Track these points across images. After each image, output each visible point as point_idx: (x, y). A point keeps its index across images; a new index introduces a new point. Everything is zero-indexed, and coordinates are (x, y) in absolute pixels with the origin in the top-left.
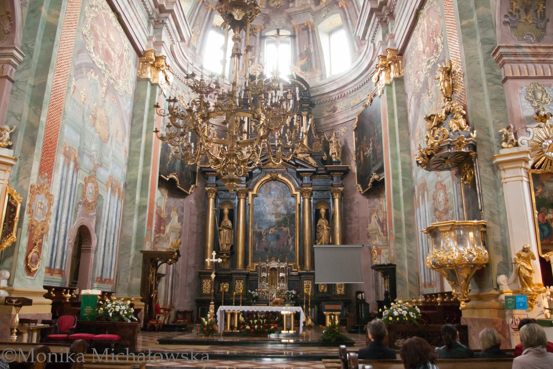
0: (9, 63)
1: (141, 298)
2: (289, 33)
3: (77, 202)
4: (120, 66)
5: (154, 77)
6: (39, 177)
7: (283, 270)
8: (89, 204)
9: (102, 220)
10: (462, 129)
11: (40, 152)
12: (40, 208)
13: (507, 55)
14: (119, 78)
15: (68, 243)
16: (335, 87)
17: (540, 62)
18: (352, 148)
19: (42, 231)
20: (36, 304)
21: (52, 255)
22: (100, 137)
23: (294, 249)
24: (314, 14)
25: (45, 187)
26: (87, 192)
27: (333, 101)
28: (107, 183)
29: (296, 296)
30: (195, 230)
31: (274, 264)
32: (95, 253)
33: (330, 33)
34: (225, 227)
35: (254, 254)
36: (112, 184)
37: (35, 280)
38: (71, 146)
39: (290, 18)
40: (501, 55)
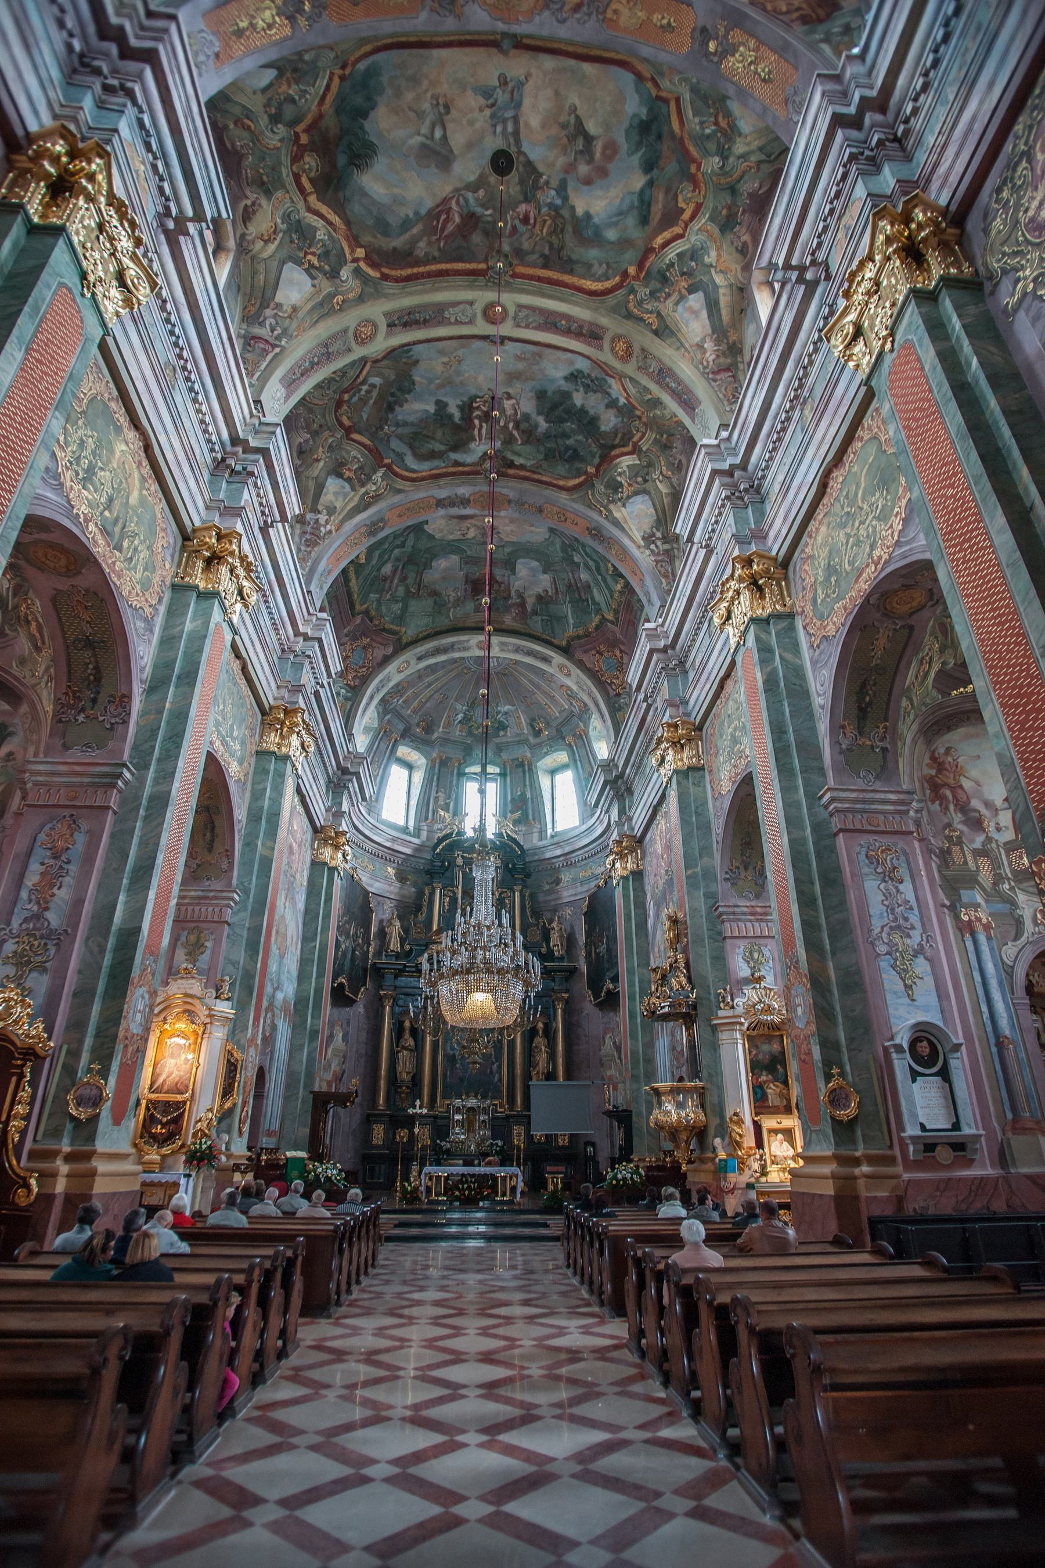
0: (228, 906)
2: (498, 770)
5: (332, 858)
7: (485, 1111)
10: (682, 988)
13: (726, 913)
16: (558, 852)
17: (757, 920)
18: (581, 939)
23: (500, 1080)
24: (532, 747)
27: (557, 870)
29: (502, 1147)
30: (363, 1052)
31: (472, 1102)
33: (553, 772)
34: (404, 1048)
35: (445, 1086)
39: (499, 749)
40: (721, 914)
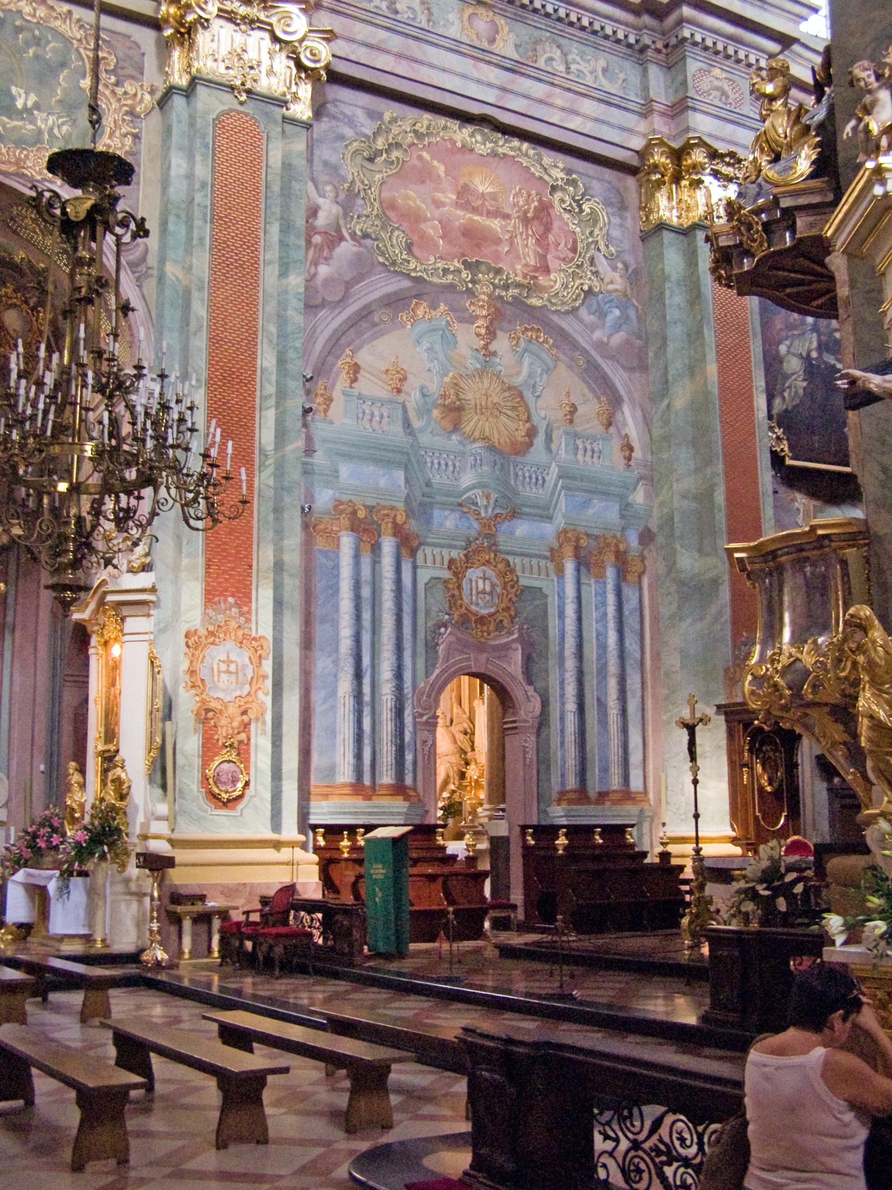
1: (733, 834)
3: (430, 624)
4: (542, 240)
6: (210, 611)
8: (482, 620)
9: (554, 648)
11: (201, 561)
12: (228, 672)
14: (547, 270)
15: (415, 724)
19: (245, 718)
20: (181, 865)
21: (359, 756)
22: (491, 448)
25: (233, 624)
26: (465, 593)
28: (552, 550)
32: (538, 734)
36: (577, 548)
37: (241, 815)
38: (371, 502)
